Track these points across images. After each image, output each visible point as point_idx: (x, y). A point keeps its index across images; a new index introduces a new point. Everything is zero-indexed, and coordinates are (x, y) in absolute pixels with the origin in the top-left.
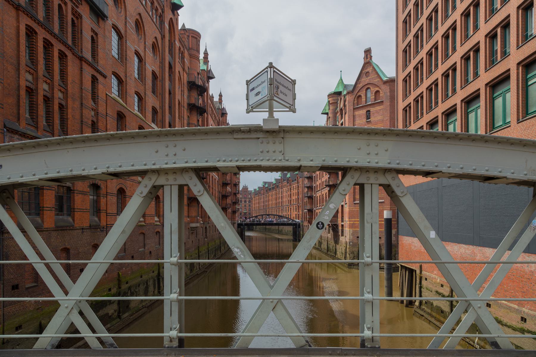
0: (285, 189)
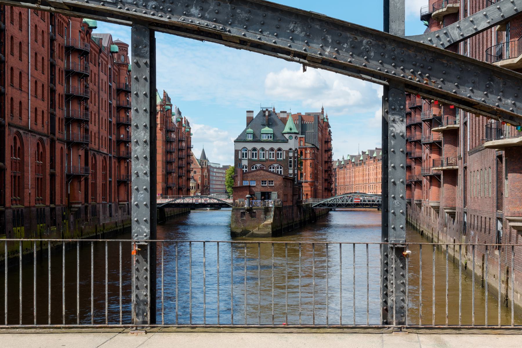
0: (371, 166)
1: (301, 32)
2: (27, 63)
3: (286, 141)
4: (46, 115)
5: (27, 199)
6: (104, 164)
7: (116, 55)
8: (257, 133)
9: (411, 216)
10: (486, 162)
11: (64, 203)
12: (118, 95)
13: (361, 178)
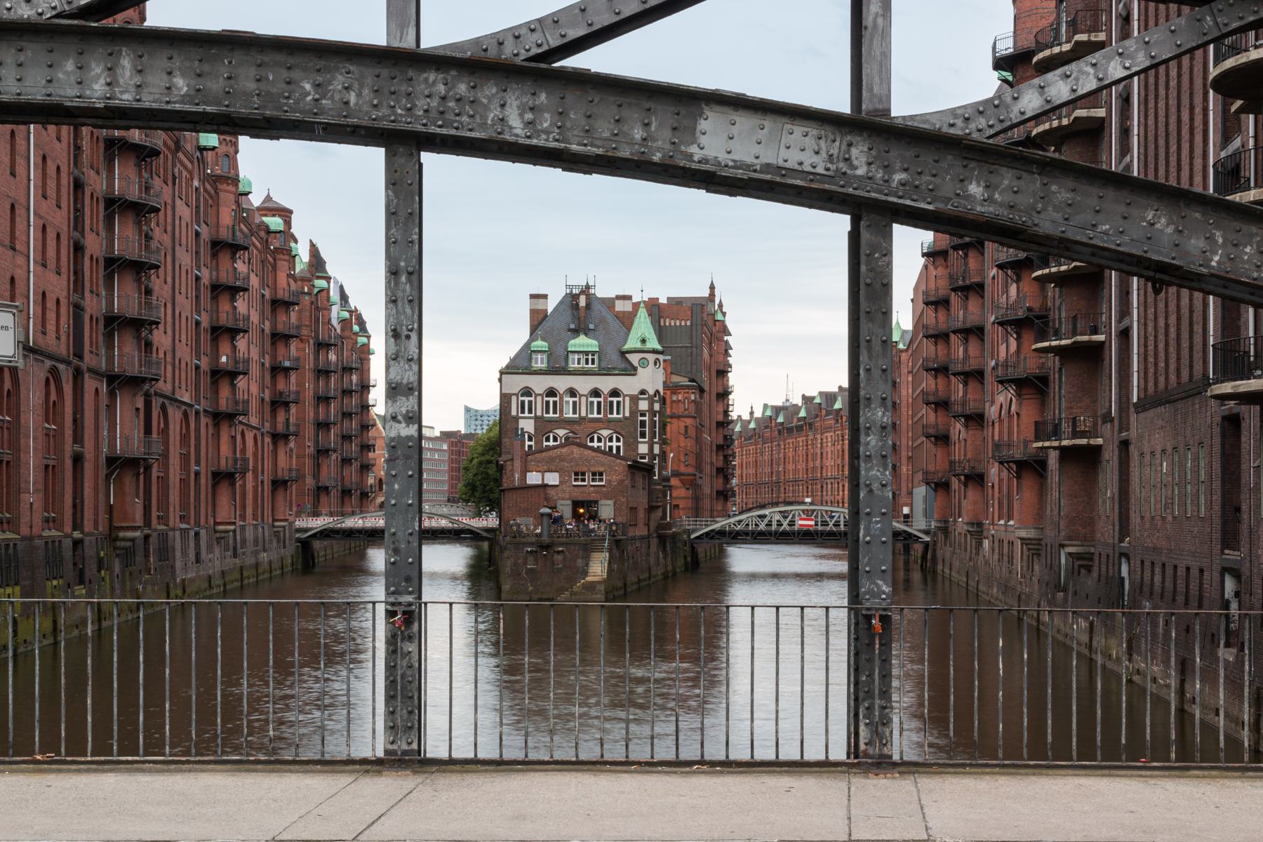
0: (829, 435)
1: (1168, 225)
2: (26, 182)
3: (631, 370)
4: (63, 310)
5: (25, 519)
7: (209, 156)
8: (560, 351)
9: (947, 564)
10: (1188, 431)
11: (101, 529)
12: (214, 255)
13: (801, 466)
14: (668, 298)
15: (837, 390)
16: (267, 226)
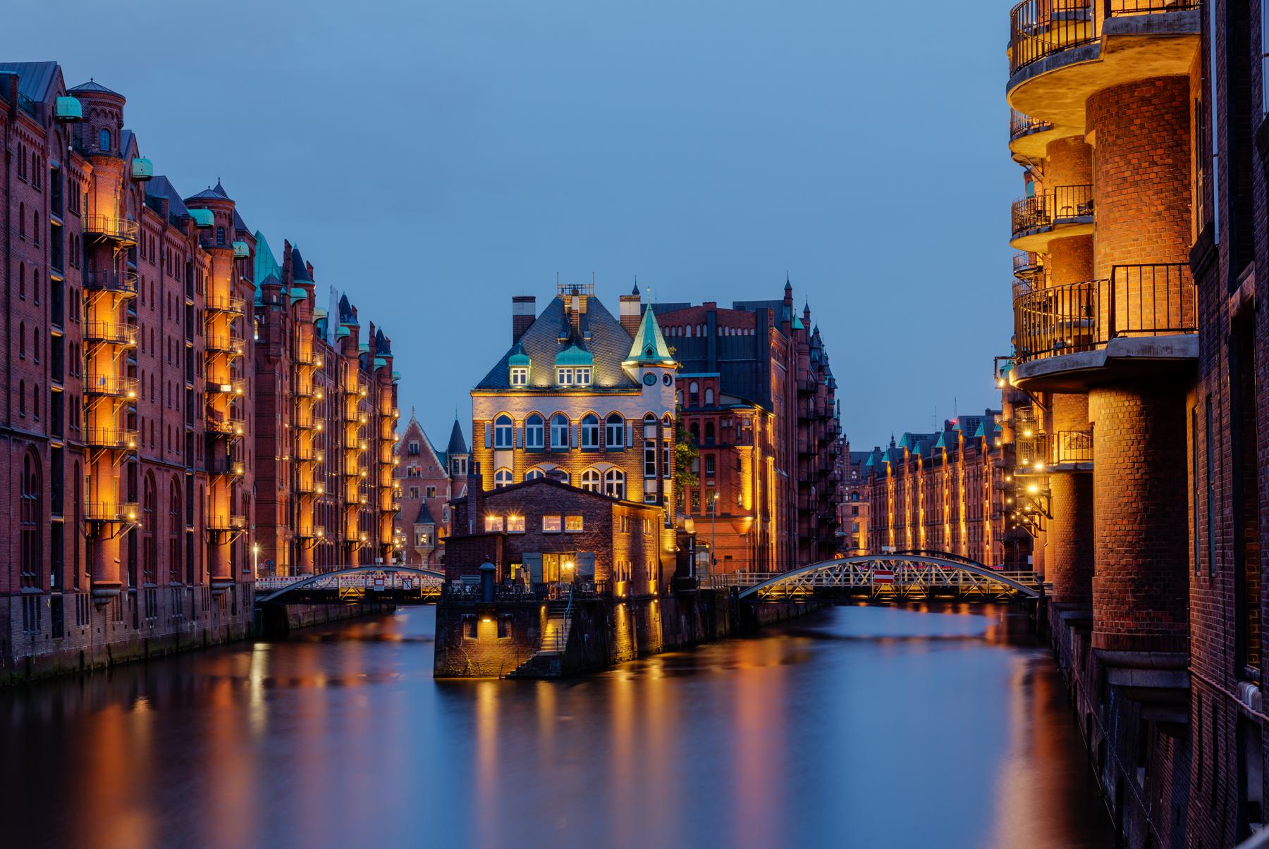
6: (32, 471)
14: (734, 303)
15: (984, 414)
16: (194, 220)
